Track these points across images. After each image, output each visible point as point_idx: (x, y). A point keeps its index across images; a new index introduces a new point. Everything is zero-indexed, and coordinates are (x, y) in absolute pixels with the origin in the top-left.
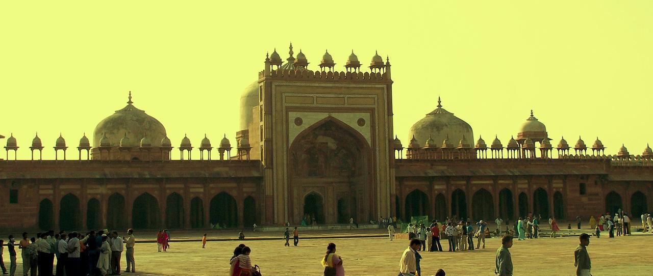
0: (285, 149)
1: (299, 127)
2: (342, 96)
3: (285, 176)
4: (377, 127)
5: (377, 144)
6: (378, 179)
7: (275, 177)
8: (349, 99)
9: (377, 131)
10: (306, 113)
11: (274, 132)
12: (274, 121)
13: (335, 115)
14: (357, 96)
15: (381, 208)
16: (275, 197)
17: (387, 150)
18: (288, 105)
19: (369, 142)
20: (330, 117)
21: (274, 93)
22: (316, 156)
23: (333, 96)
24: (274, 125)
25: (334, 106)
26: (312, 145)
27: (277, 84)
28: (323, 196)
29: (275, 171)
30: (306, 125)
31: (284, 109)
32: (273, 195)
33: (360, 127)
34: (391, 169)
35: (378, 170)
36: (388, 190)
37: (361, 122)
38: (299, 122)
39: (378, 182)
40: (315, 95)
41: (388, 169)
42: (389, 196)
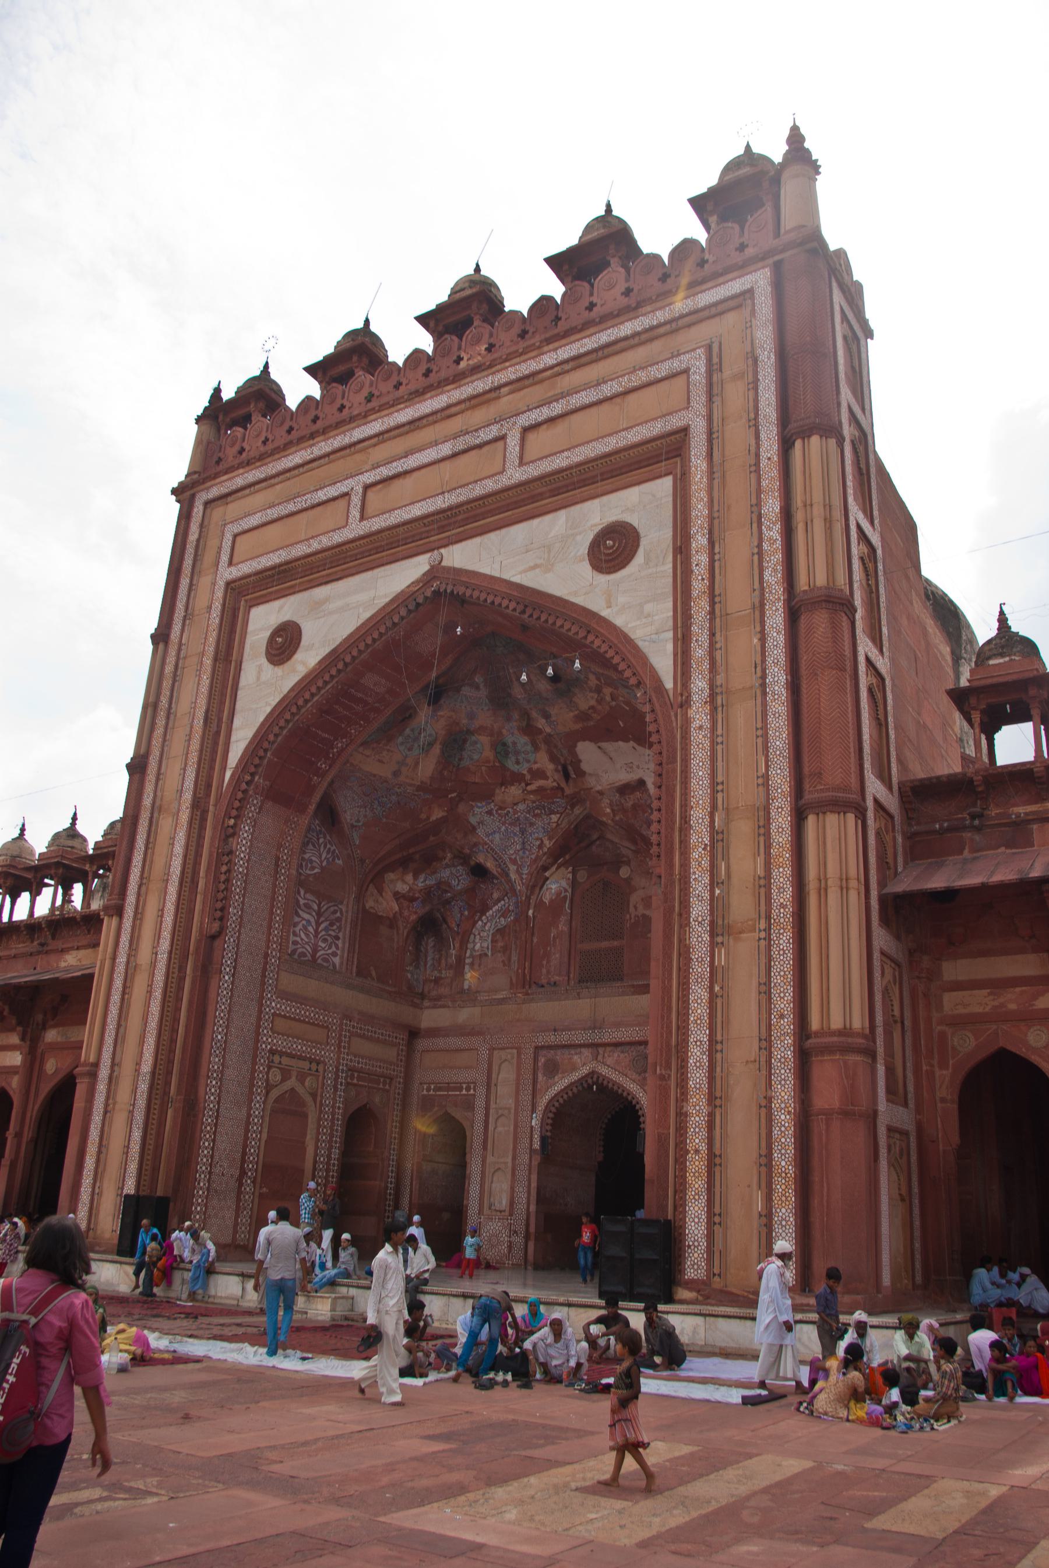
0: (188, 796)
1: (279, 671)
2: (493, 431)
3: (165, 945)
4: (699, 540)
5: (699, 652)
6: (699, 910)
7: (122, 959)
8: (531, 437)
9: (700, 560)
10: (320, 592)
11: (161, 722)
12: (169, 669)
13: (464, 556)
14: (577, 400)
15: (714, 1161)
16: (104, 1073)
17: (778, 678)
18: (234, 572)
19: (662, 662)
20: (435, 572)
21: (193, 537)
22: (624, 872)
23: (446, 449)
24: (166, 684)
25: (440, 503)
26: (577, 810)
27: (215, 492)
28: (643, 1098)
29: (127, 923)
30: (308, 658)
31: (219, 594)
32: (96, 1065)
33: (603, 579)
34: (811, 821)
35: (699, 836)
36: (784, 1000)
37: (613, 549)
38: (284, 643)
39: (699, 937)
40: (355, 485)
41: (781, 821)
42: (784, 1050)
